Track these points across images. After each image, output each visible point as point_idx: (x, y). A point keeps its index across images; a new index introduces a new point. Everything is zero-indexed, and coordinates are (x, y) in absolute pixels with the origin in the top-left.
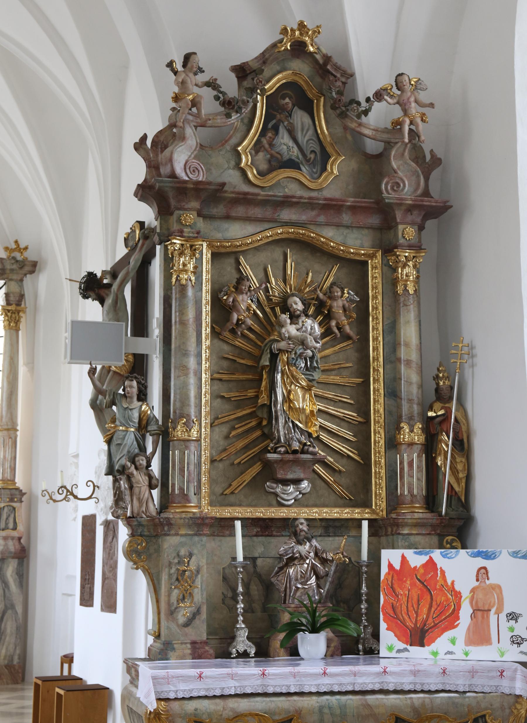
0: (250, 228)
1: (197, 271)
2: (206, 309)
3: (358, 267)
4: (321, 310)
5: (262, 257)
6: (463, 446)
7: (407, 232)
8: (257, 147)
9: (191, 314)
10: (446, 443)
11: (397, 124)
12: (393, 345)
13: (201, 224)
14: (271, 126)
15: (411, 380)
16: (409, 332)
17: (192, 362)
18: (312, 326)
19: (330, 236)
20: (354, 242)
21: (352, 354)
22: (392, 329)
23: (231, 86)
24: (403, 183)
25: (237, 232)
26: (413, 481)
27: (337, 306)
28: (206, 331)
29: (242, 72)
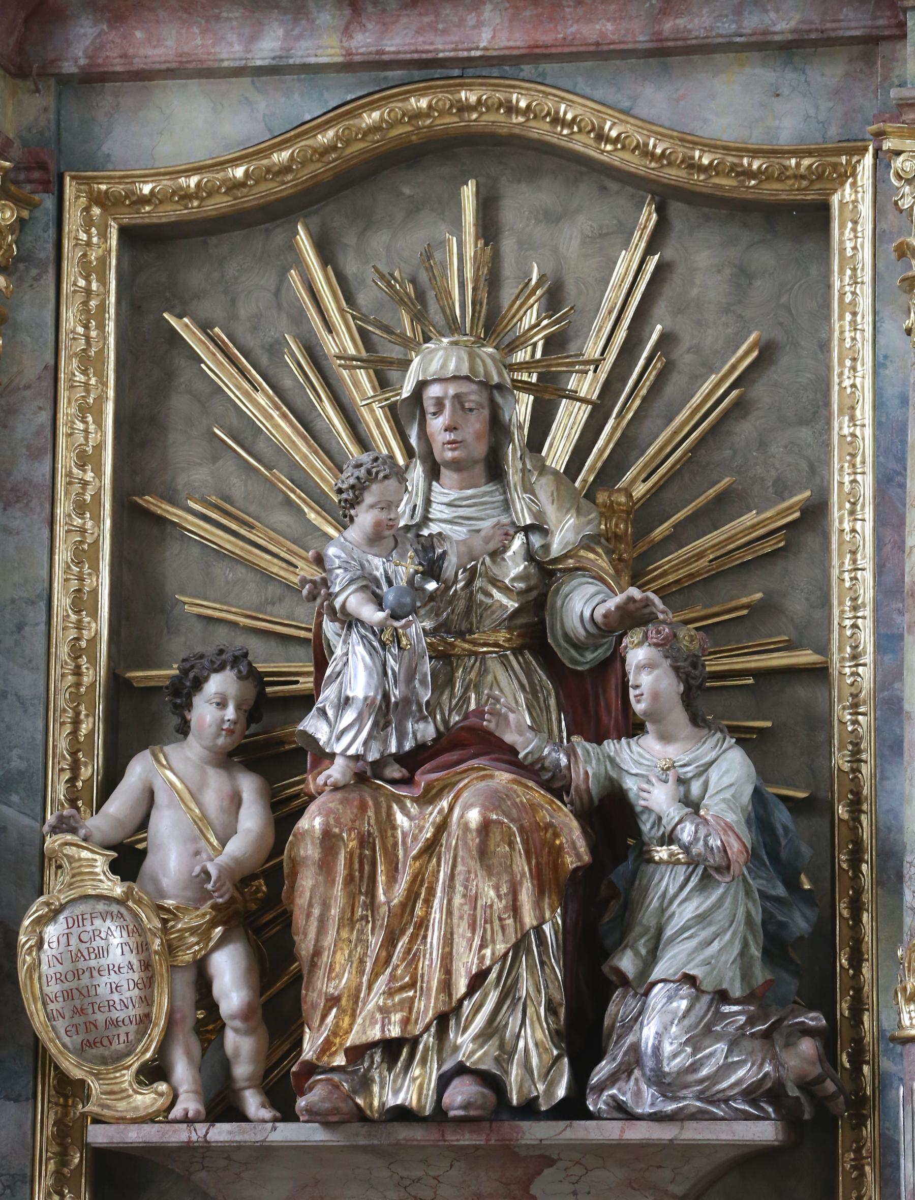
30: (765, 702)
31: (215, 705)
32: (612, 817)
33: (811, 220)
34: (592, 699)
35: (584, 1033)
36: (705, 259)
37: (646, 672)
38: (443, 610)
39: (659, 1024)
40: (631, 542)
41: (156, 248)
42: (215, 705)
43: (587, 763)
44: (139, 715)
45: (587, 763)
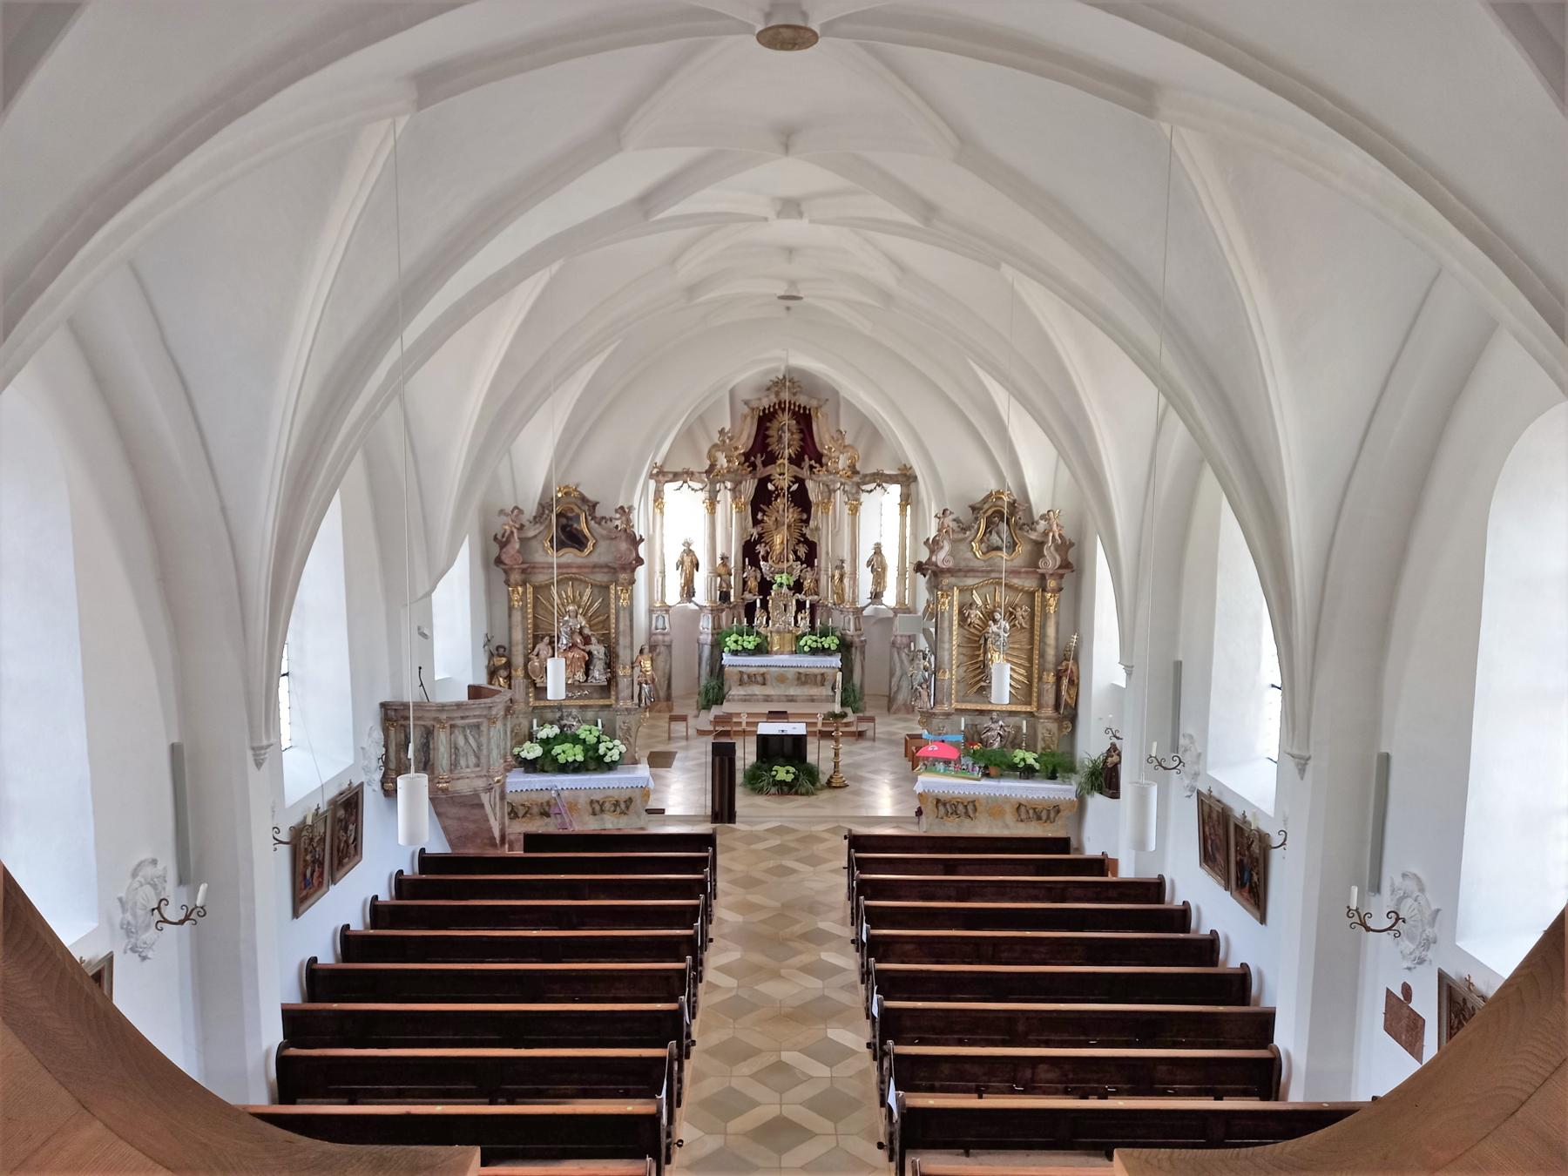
0: (977, 581)
1: (951, 604)
2: (955, 618)
3: (1032, 594)
4: (1011, 616)
5: (984, 590)
6: (1074, 683)
7: (1052, 584)
8: (981, 541)
9: (946, 624)
10: (1065, 681)
11: (1045, 534)
12: (1043, 635)
13: (953, 580)
14: (988, 531)
15: (1051, 653)
16: (1051, 631)
17: (947, 646)
18: (1005, 624)
19: (1015, 581)
20: (1030, 583)
21: (1027, 634)
22: (1043, 626)
23: (966, 516)
24: (1051, 561)
25: (970, 581)
26: (1050, 698)
27: (1019, 613)
28: (955, 627)
29: (973, 508)
30: (606, 640)
31: (547, 640)
32: (590, 653)
33: (607, 588)
34: (587, 640)
35: (587, 674)
36: (596, 591)
37: (594, 640)
38: (573, 632)
39: (596, 674)
40: (589, 621)
41: (536, 589)
42: (547, 640)
43: (588, 648)
44: (537, 639)
45: (588, 648)
